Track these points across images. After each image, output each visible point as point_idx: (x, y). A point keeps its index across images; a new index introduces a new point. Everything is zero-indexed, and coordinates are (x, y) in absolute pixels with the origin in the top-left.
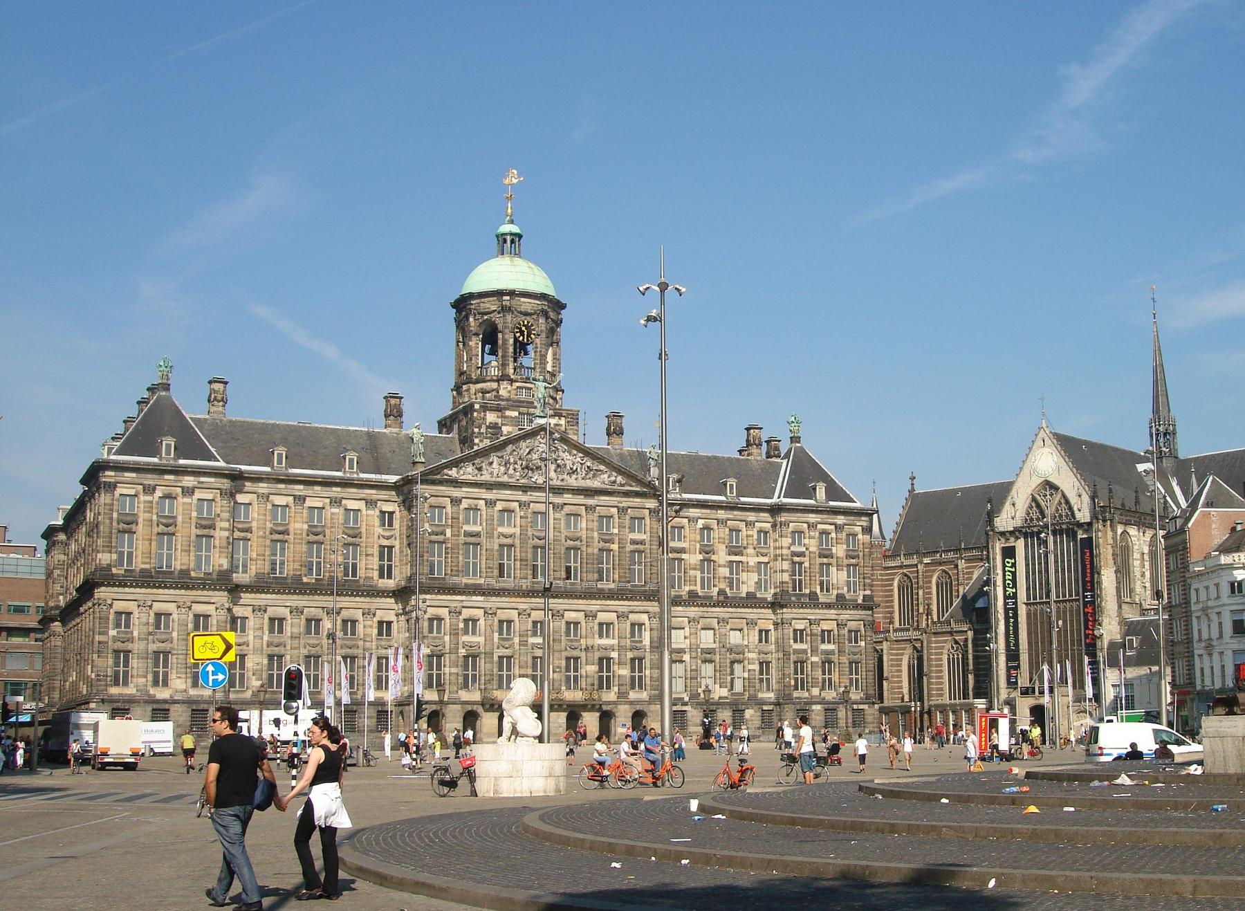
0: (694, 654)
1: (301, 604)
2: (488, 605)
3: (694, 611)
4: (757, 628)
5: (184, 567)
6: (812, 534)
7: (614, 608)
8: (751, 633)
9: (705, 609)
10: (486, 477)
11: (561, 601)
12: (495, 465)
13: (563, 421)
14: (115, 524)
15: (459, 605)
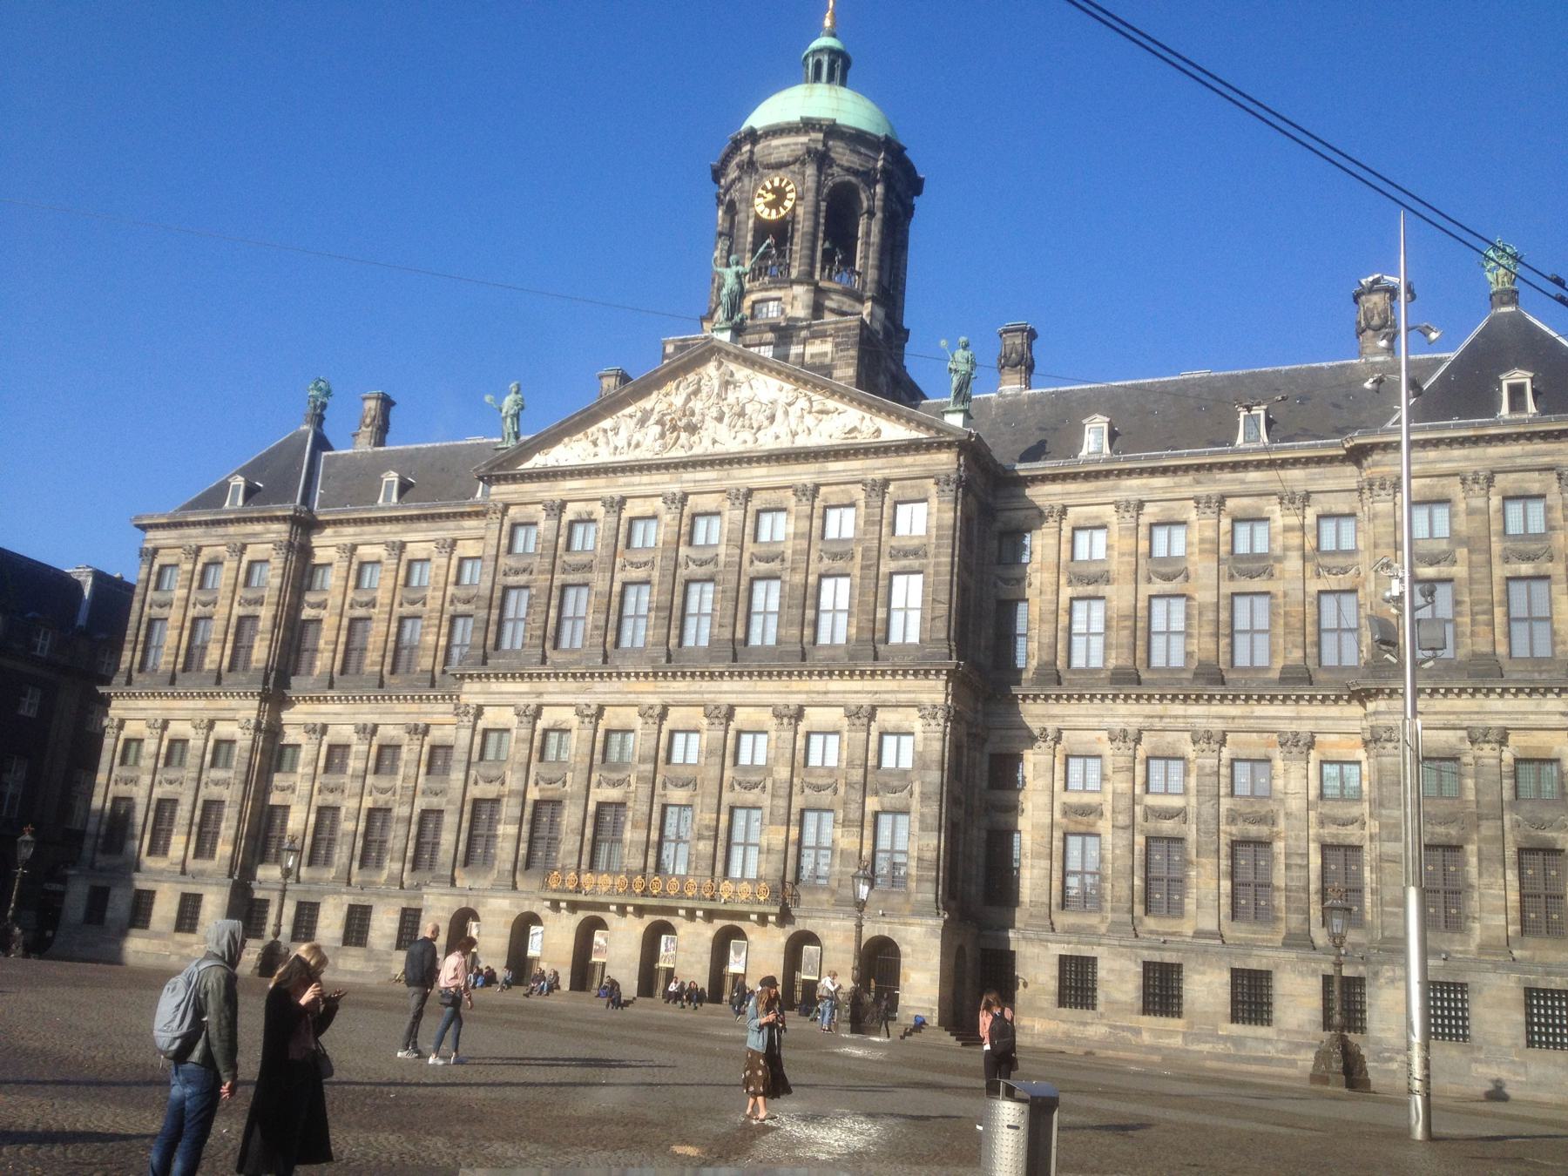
0: (1123, 819)
1: (375, 719)
2: (582, 699)
3: (1126, 714)
4: (1314, 755)
5: (214, 666)
6: (1479, 503)
7: (839, 698)
8: (1296, 769)
9: (1157, 708)
10: (605, 456)
11: (726, 685)
12: (623, 433)
13: (827, 347)
14: (146, 609)
15: (533, 701)
